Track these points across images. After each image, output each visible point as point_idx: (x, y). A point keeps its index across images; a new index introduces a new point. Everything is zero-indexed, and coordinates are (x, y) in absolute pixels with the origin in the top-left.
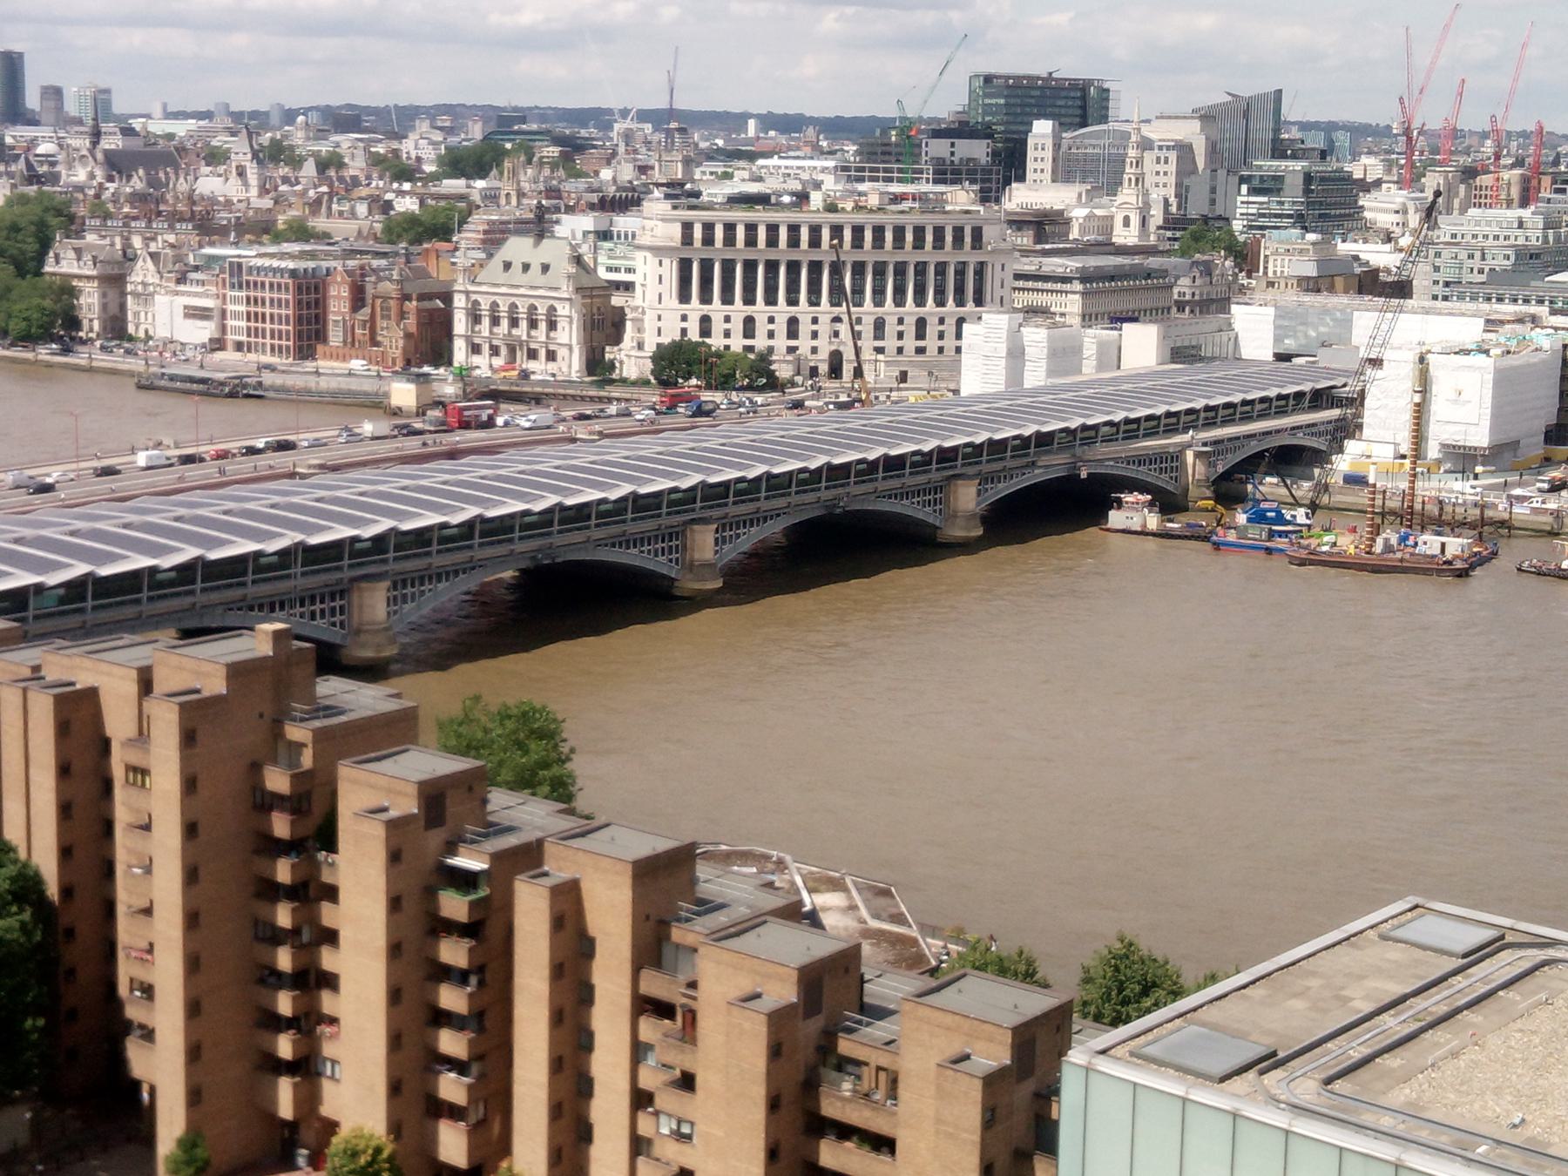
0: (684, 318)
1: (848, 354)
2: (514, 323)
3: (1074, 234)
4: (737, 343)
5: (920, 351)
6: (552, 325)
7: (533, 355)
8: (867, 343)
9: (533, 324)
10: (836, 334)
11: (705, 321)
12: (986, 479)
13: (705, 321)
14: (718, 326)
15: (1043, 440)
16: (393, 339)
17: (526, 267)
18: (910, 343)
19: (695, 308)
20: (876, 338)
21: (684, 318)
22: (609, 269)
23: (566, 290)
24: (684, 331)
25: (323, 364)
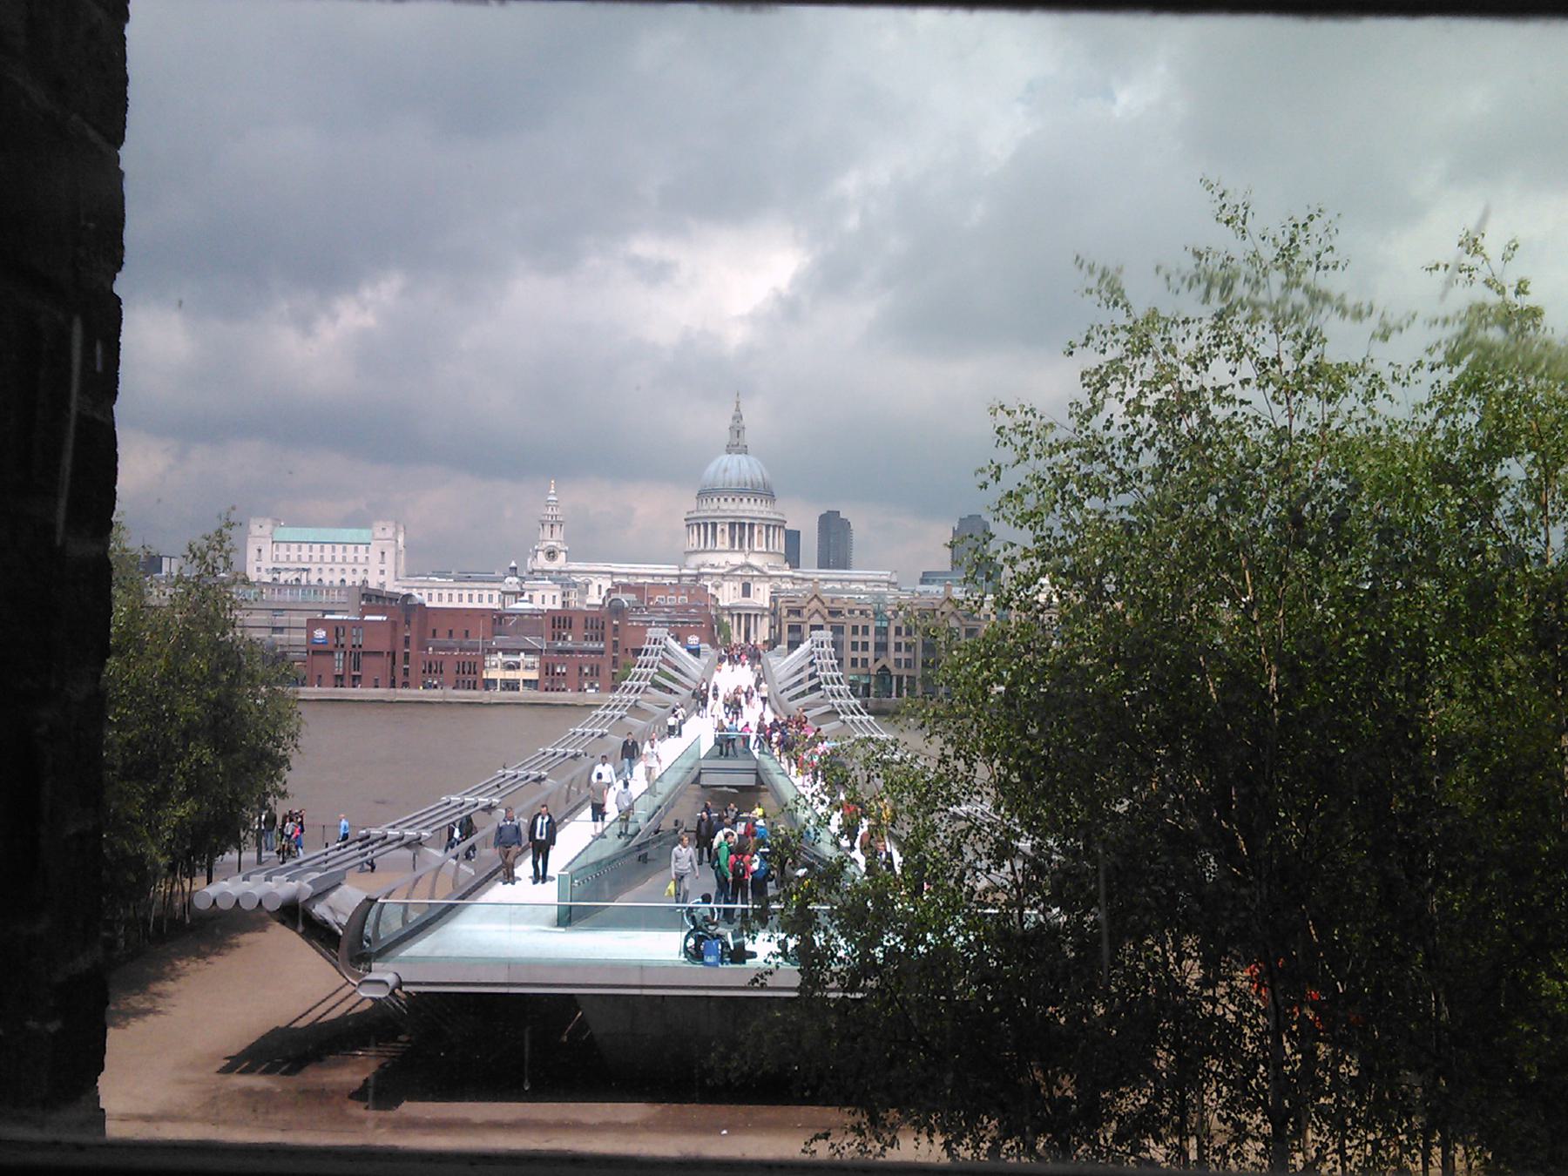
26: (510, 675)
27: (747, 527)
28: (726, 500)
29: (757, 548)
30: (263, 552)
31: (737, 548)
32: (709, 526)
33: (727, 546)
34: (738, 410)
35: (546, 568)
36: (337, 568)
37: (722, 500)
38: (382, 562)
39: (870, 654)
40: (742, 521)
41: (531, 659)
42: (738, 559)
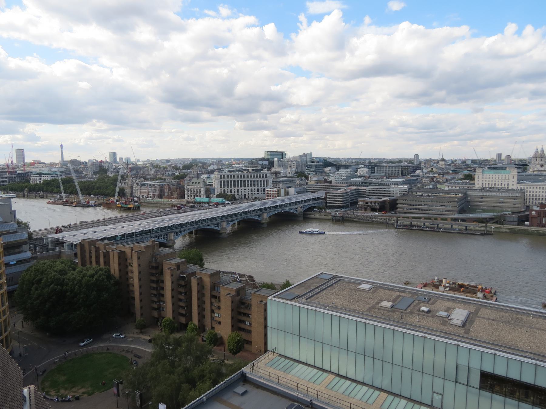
0: (221, 190)
1: (247, 194)
2: (194, 192)
3: (282, 175)
4: (229, 193)
5: (258, 194)
6: (200, 192)
7: (197, 196)
8: (250, 193)
9: (197, 192)
10: (245, 191)
11: (224, 191)
12: (268, 213)
13: (224, 191)
14: (226, 191)
15: (277, 206)
16: (175, 195)
17: (196, 183)
18: (256, 192)
19: (223, 189)
20: (251, 192)
21: (221, 190)
22: (209, 183)
23: (202, 186)
24: (221, 192)
25: (163, 200)
36: (500, 180)
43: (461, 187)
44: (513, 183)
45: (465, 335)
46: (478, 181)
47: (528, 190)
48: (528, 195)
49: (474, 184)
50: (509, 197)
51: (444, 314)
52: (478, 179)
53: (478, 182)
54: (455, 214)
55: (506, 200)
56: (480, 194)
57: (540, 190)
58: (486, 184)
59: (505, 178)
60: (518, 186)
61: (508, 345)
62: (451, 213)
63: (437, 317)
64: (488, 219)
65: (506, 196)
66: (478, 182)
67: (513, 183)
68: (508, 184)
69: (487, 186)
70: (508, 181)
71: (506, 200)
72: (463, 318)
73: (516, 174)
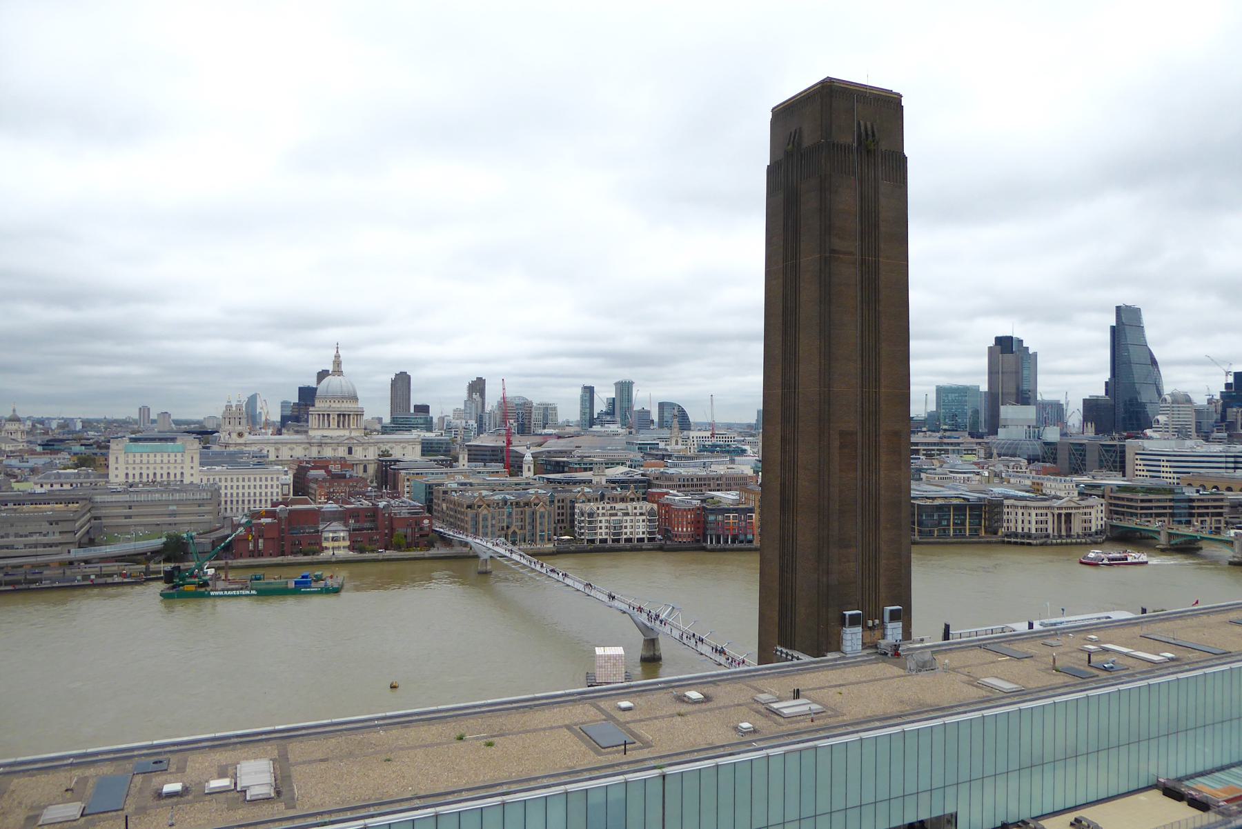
26: (336, 544)
27: (347, 417)
28: (334, 402)
29: (352, 427)
30: (119, 459)
31: (342, 427)
32: (326, 416)
33: (336, 427)
34: (337, 352)
35: (237, 442)
36: (165, 467)
37: (332, 401)
38: (192, 462)
39: (505, 525)
40: (345, 413)
41: (342, 534)
42: (346, 433)
43: (84, 485)
44: (193, 472)
45: (291, 813)
46: (117, 469)
47: (223, 484)
48: (223, 495)
49: (107, 476)
50: (189, 502)
51: (225, 782)
52: (116, 466)
53: (116, 472)
54: (69, 552)
55: (182, 509)
56: (126, 497)
57: (267, 483)
58: (134, 475)
59: (176, 460)
60: (202, 477)
61: (377, 799)
62: (59, 548)
63: (208, 798)
64: (149, 554)
65: (183, 500)
66: (116, 472)
67: (193, 472)
68: (182, 473)
69: (137, 480)
70: (182, 468)
71: (182, 509)
72: (268, 778)
73: (195, 453)
